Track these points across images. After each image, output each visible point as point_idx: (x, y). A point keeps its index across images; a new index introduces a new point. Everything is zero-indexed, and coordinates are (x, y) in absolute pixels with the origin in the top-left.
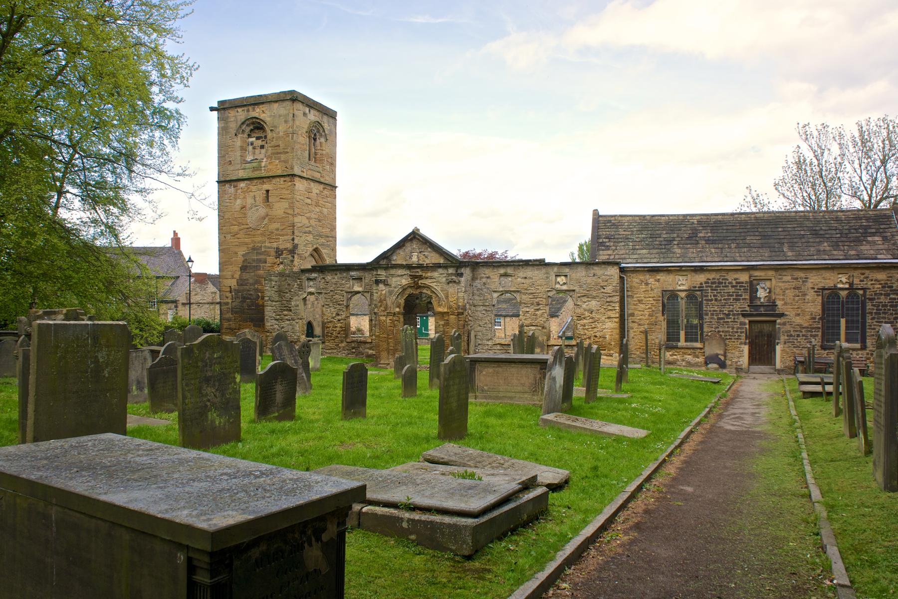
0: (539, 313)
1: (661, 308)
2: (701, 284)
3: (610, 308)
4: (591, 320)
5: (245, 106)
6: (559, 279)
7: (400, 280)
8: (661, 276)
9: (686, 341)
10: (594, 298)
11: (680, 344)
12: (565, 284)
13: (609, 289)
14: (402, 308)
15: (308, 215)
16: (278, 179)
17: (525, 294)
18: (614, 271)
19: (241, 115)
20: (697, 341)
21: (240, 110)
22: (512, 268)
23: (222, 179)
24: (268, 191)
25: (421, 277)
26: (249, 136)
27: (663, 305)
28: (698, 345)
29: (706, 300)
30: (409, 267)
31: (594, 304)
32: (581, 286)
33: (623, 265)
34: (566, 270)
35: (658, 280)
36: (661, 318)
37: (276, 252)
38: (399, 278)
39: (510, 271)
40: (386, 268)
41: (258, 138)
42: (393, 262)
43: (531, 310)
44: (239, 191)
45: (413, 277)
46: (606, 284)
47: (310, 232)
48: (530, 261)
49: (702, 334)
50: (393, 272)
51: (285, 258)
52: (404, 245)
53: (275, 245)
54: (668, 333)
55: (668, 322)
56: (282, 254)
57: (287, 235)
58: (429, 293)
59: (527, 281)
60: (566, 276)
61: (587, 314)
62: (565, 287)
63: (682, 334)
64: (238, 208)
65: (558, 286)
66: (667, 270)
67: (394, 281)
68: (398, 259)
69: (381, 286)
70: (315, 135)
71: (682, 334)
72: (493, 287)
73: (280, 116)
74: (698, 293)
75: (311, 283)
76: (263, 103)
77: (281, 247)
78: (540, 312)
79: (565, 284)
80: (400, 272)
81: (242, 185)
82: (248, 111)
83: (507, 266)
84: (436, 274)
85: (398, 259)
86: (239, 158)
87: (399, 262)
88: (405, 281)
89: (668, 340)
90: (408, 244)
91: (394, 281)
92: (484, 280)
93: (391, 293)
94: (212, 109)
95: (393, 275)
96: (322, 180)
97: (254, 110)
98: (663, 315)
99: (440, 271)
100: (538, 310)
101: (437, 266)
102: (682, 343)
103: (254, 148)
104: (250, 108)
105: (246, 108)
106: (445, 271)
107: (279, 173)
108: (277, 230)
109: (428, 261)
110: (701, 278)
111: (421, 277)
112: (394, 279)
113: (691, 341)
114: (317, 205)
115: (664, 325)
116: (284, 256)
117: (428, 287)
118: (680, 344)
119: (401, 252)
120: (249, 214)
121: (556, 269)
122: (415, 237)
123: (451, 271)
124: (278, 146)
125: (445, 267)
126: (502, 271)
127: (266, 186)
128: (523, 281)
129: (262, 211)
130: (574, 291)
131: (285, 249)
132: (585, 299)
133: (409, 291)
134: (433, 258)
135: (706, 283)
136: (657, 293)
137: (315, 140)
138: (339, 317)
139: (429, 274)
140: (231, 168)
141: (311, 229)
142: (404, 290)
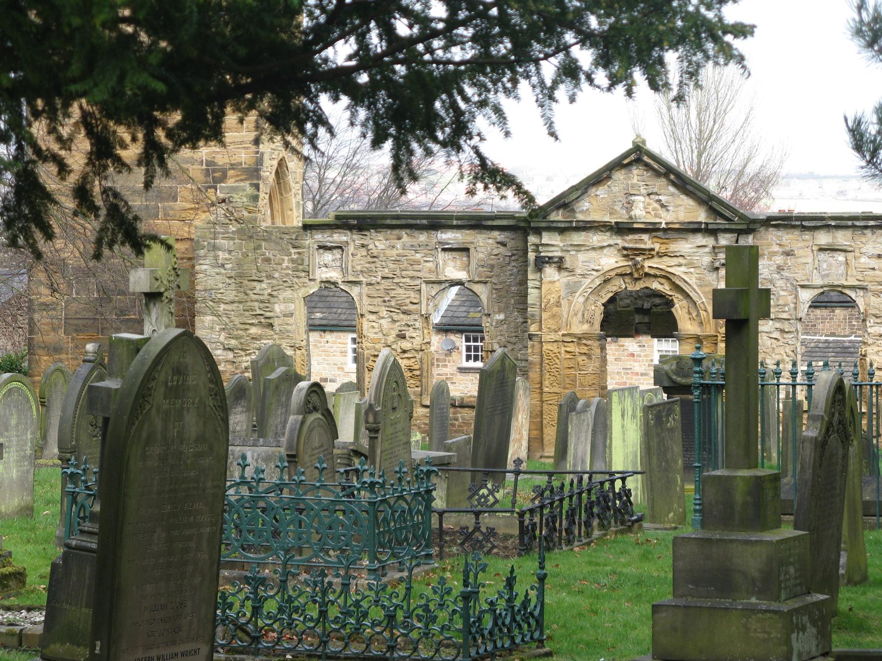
22: (848, 233)
25: (649, 253)
30: (621, 229)
37: (207, 173)
38: (593, 254)
39: (842, 238)
40: (562, 230)
42: (580, 217)
45: (629, 253)
50: (577, 238)
51: (234, 189)
52: (609, 177)
56: (224, 178)
58: (664, 288)
67: (580, 261)
68: (590, 208)
69: (550, 272)
72: (800, 277)
75: (328, 257)
80: (596, 239)
83: (837, 227)
85: (590, 208)
87: (596, 217)
88: (610, 261)
90: (619, 175)
91: (580, 261)
92: (779, 260)
93: (572, 289)
95: (578, 247)
99: (700, 240)
101: (693, 229)
106: (710, 241)
111: (649, 253)
112: (582, 257)
116: (230, 183)
117: (667, 277)
119: (601, 191)
122: (637, 157)
123: (725, 240)
125: (712, 232)
126: (823, 238)
131: (233, 166)
133: (618, 285)
138: (406, 345)
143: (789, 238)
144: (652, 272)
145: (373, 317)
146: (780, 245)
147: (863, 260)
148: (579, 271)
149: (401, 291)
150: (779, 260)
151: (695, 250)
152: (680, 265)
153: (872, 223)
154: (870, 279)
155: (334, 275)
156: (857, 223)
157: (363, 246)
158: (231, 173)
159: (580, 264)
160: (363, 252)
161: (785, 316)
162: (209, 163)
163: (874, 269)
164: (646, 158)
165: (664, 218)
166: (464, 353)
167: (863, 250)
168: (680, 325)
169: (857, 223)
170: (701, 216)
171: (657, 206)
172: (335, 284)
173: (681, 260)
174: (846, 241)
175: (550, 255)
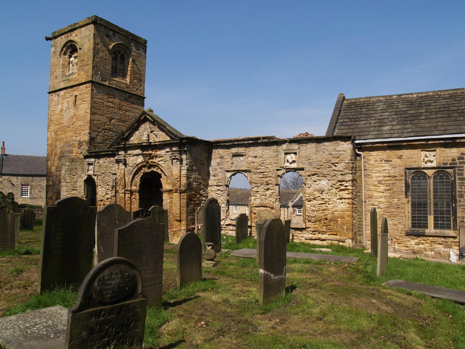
0: (268, 193)
1: (404, 189)
2: (454, 160)
3: (343, 188)
4: (321, 202)
5: (65, 33)
6: (289, 157)
7: (135, 159)
8: (405, 153)
9: (436, 227)
10: (324, 176)
11: (427, 231)
12: (294, 162)
13: (341, 166)
14: (138, 187)
15: (110, 115)
16: (82, 86)
17: (255, 173)
18: (346, 147)
19: (62, 41)
20: (449, 228)
21: (63, 37)
23: (51, 90)
24: (76, 96)
25: (151, 157)
26: (70, 57)
27: (407, 186)
28: (451, 233)
29: (459, 179)
31: (324, 183)
32: (310, 164)
33: (357, 142)
34: (295, 146)
35: (400, 157)
36: (405, 200)
37: (79, 144)
38: (135, 158)
39: (241, 150)
41: (75, 57)
42: (131, 143)
43: (261, 189)
44: (60, 98)
46: (337, 160)
47: (110, 130)
48: (259, 139)
49: (455, 220)
50: (129, 152)
53: (78, 138)
54: (413, 218)
55: (413, 205)
57: (86, 130)
58: (159, 171)
59: (257, 160)
60: (295, 153)
61: (317, 194)
62: (294, 166)
63: (431, 219)
64: (58, 111)
65: (287, 164)
66: (410, 146)
70: (122, 55)
71: (431, 219)
72: (226, 167)
73: (86, 37)
74: (449, 171)
76: (76, 29)
77: (82, 140)
78: (270, 192)
79: (294, 162)
81: (62, 93)
82: (68, 36)
84: (163, 152)
86: (61, 73)
88: (140, 159)
89: (413, 225)
92: (218, 160)
94: (48, 39)
96: (126, 90)
97: (71, 35)
98: (406, 196)
100: (268, 189)
102: (431, 230)
103: (73, 66)
104: (69, 34)
105: (66, 35)
107: (83, 81)
108: (80, 126)
109: (157, 140)
110: (454, 153)
113: (442, 227)
114: (120, 109)
115: (408, 208)
118: (427, 231)
120: (65, 115)
121: (284, 146)
124: (84, 60)
126: (234, 150)
127: (76, 93)
128: (254, 160)
129: (72, 111)
130: (302, 169)
131: (84, 141)
132: (315, 178)
134: (163, 137)
135: (459, 158)
136: (399, 171)
137: (124, 59)
138: (108, 196)
139: (158, 153)
140: (57, 81)
141: (111, 127)
142: (140, 169)
143: (221, 151)
144: (152, 164)
145: (100, 187)
146: (219, 154)
147: (250, 159)
148: (130, 165)
149: (107, 177)
150: (218, 160)
151: (166, 153)
152: (162, 160)
153: (251, 142)
154: (252, 167)
155: (91, 173)
156: (245, 142)
157: (98, 162)
158: (84, 143)
159: (131, 162)
160: (98, 165)
161: (221, 184)
162: (80, 141)
163: (254, 162)
164: (148, 117)
165: (154, 139)
166: (298, 211)
167: (249, 154)
168: (163, 187)
169: (245, 142)
170: (168, 139)
171: (154, 136)
172: (91, 176)
173: (162, 158)
174: (243, 151)
175: (121, 158)
